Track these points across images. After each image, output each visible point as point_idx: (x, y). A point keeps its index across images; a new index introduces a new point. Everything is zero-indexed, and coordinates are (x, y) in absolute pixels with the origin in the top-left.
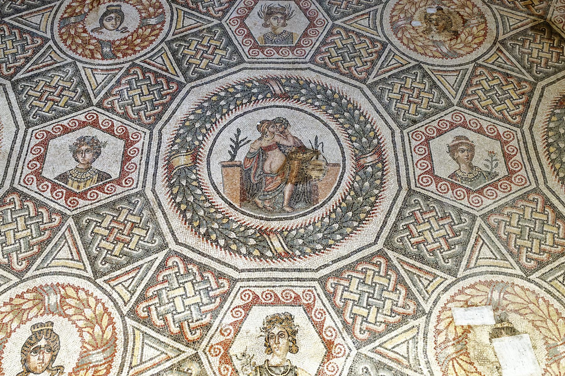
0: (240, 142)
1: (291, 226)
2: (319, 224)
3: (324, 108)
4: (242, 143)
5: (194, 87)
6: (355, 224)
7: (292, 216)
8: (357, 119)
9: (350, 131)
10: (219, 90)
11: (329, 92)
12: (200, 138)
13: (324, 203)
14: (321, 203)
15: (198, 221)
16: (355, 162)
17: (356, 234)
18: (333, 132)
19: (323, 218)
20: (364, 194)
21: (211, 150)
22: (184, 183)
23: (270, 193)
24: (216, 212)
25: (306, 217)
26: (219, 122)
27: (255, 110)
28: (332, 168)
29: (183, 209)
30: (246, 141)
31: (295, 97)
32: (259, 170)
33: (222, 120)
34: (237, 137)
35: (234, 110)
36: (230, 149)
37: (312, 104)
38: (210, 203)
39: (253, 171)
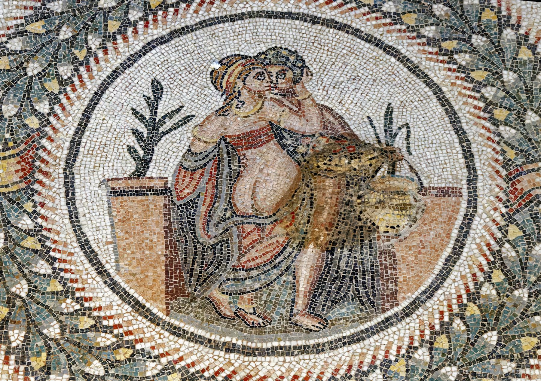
0: (162, 122)
4: (169, 123)
6: (508, 367)
7: (321, 341)
8: (508, 55)
9: (489, 92)
12: (43, 107)
13: (415, 305)
14: (404, 304)
15: (44, 355)
16: (504, 185)
18: (438, 92)
19: (412, 348)
20: (533, 279)
21: (75, 145)
23: (255, 273)
24: (95, 328)
25: (362, 344)
26: (97, 61)
27: (203, 24)
28: (437, 200)
30: (178, 118)
32: (221, 205)
33: (106, 53)
34: (153, 104)
35: (141, 23)
36: (132, 141)
38: (77, 300)
39: (202, 209)
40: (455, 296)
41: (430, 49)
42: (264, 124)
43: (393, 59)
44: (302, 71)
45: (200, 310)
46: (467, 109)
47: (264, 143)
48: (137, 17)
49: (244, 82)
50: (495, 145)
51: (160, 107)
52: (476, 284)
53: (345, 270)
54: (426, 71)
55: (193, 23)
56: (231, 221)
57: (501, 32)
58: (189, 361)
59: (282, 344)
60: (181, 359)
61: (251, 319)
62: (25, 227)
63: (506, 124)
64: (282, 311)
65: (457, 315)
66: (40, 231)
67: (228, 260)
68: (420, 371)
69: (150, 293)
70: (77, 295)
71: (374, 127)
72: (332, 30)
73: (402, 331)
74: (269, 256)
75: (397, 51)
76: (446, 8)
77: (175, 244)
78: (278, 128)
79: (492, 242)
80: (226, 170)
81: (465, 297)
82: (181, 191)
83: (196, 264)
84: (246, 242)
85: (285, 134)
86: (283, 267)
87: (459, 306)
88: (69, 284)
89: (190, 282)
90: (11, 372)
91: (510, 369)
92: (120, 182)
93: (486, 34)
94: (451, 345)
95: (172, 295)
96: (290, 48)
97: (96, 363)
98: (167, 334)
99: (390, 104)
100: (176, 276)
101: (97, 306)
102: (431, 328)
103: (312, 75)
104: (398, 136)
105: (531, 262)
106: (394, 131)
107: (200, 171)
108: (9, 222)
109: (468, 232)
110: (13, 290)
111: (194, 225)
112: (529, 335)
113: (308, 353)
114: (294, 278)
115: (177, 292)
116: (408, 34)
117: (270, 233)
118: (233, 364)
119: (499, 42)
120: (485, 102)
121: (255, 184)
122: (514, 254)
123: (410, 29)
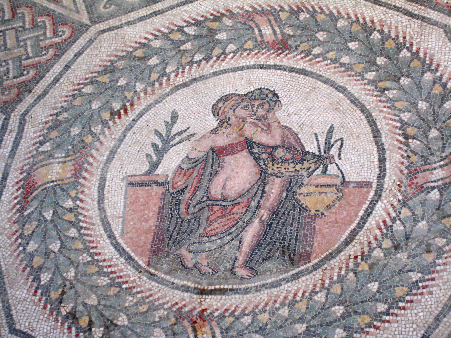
0: (173, 138)
1: (242, 306)
2: (302, 306)
3: (359, 68)
4: (177, 139)
5: (104, 31)
6: (381, 307)
7: (249, 285)
10: (151, 37)
11: (376, 36)
17: (377, 328)
19: (314, 292)
20: (413, 246)
22: (48, 215)
23: (214, 238)
26: (139, 98)
27: (215, 74)
29: (35, 266)
30: (184, 135)
31: (304, 46)
36: (151, 151)
37: (334, 61)
38: (91, 255)
40: (352, 257)
41: (369, 88)
42: (242, 139)
43: (341, 95)
44: (276, 104)
45: (171, 263)
46: (388, 127)
47: (239, 152)
48: (171, 70)
49: (234, 111)
50: (403, 153)
51: (174, 129)
52: (370, 249)
53: (277, 238)
54: (363, 102)
55: (208, 73)
56: (205, 203)
57: (423, 74)
58: (156, 297)
59: (222, 287)
60: (151, 295)
61: (204, 270)
62: (68, 207)
63: (414, 138)
64: (228, 265)
65: (352, 270)
66: (77, 209)
67: (198, 229)
68: (316, 309)
69: (140, 249)
70: (92, 251)
71: (317, 140)
72: (302, 76)
73: (309, 280)
74: (226, 227)
75: (345, 89)
76: (385, 60)
77: (164, 218)
78: (251, 141)
79: (388, 220)
80: (209, 169)
81: (360, 257)
82: (176, 184)
83: (175, 233)
84: (213, 217)
85: (255, 146)
86: (234, 234)
87: (354, 264)
88: (88, 244)
89: (168, 244)
90: (36, 301)
91: (383, 309)
92: (137, 177)
93: (412, 77)
94: (342, 291)
95: (155, 252)
96: (270, 89)
97: (94, 296)
98: (145, 278)
99: (332, 125)
100: (159, 240)
101: (103, 258)
102: (330, 279)
103: (282, 106)
104: (334, 147)
105: (414, 235)
106: (332, 143)
107: (191, 171)
108: (58, 203)
109: (371, 213)
110: (51, 247)
111: (179, 206)
112: (403, 286)
113: (238, 293)
114: (240, 242)
115: (158, 251)
116: (355, 78)
117: (230, 212)
118: (185, 300)
119: (420, 82)
120: (401, 123)
121: (227, 179)
122: (402, 228)
123: (358, 74)
